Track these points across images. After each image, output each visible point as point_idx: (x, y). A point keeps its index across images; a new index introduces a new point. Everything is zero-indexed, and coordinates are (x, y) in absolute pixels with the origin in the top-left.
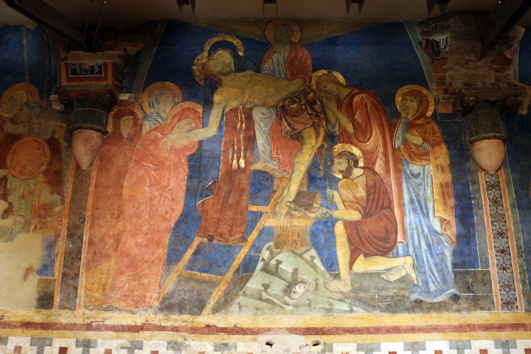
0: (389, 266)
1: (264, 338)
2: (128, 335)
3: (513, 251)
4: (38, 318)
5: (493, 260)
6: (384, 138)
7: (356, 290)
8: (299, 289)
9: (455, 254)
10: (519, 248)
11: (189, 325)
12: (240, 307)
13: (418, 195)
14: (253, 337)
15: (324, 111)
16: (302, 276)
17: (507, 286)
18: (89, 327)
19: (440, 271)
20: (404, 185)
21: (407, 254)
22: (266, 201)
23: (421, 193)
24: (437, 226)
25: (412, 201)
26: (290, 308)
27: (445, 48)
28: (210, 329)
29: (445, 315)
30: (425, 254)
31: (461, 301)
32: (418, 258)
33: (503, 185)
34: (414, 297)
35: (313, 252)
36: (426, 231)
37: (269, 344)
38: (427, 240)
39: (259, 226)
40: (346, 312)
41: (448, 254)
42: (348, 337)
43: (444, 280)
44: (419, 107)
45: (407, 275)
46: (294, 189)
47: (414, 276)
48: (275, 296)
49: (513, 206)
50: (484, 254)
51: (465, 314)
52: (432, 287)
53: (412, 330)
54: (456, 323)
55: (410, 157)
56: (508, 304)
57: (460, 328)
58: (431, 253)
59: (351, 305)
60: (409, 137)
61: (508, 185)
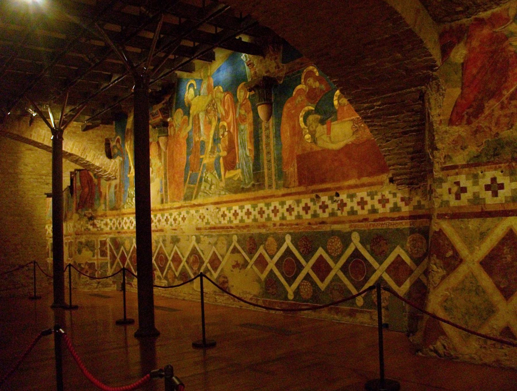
0: (234, 174)
1: (206, 207)
2: (178, 210)
3: (272, 161)
4: (161, 208)
5: (265, 167)
6: (233, 115)
7: (227, 185)
8: (213, 187)
9: (254, 165)
10: (275, 158)
11: (190, 204)
12: (200, 196)
13: (243, 140)
14: (203, 207)
15: (217, 108)
16: (214, 182)
17: (270, 178)
18: (171, 209)
19: (249, 174)
20: (239, 136)
21: (239, 168)
22: (203, 154)
23: (244, 139)
24: (248, 154)
25: (241, 144)
26: (211, 195)
27: (246, 60)
28: (194, 206)
29: (250, 193)
30: (245, 167)
31: (255, 186)
32: (243, 169)
33: (271, 126)
34: (242, 186)
35: (215, 172)
36: (245, 156)
37: (207, 209)
38: (245, 160)
39: (202, 164)
40: (224, 195)
41: (251, 165)
42: (225, 204)
43: (250, 178)
44: (244, 94)
45: (240, 177)
46: (210, 146)
47: (241, 177)
48: (207, 191)
49: (274, 137)
50: (263, 164)
51: (256, 192)
52: (247, 182)
53: (241, 200)
54: (253, 197)
55: (241, 122)
56: (270, 186)
57: (254, 199)
58: (246, 167)
59: (225, 192)
60: (241, 111)
61: (272, 126)
